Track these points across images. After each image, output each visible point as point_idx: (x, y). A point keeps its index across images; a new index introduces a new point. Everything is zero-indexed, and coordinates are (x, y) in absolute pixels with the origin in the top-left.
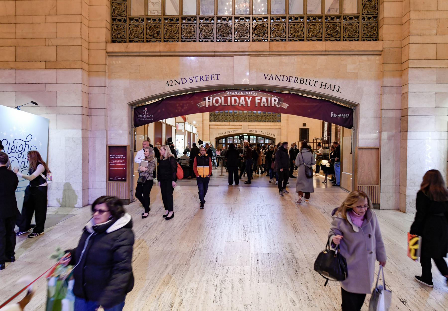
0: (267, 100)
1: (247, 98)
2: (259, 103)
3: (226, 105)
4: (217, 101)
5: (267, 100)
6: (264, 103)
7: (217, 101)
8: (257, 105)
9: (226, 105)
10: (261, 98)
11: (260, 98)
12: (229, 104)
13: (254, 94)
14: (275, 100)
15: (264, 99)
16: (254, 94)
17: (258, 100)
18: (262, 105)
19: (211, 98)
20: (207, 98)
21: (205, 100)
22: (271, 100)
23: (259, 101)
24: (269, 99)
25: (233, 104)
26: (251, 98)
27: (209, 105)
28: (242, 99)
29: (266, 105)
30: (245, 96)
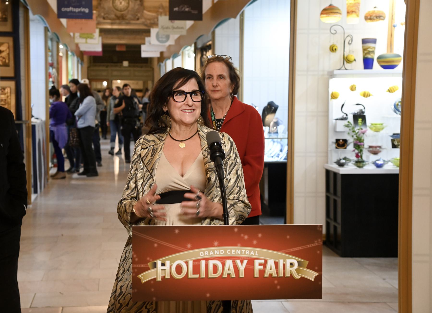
0: (277, 264)
1: (238, 262)
2: (262, 272)
4: (179, 269)
5: (277, 264)
6: (271, 272)
7: (179, 269)
8: (257, 275)
9: (197, 276)
10: (266, 261)
11: (263, 261)
13: (252, 253)
14: (292, 265)
15: (271, 263)
16: (252, 253)
17: (260, 264)
18: (267, 275)
19: (168, 263)
20: (159, 263)
21: (155, 266)
22: (284, 265)
23: (261, 267)
26: (245, 262)
27: (163, 278)
28: (229, 263)
30: (234, 258)
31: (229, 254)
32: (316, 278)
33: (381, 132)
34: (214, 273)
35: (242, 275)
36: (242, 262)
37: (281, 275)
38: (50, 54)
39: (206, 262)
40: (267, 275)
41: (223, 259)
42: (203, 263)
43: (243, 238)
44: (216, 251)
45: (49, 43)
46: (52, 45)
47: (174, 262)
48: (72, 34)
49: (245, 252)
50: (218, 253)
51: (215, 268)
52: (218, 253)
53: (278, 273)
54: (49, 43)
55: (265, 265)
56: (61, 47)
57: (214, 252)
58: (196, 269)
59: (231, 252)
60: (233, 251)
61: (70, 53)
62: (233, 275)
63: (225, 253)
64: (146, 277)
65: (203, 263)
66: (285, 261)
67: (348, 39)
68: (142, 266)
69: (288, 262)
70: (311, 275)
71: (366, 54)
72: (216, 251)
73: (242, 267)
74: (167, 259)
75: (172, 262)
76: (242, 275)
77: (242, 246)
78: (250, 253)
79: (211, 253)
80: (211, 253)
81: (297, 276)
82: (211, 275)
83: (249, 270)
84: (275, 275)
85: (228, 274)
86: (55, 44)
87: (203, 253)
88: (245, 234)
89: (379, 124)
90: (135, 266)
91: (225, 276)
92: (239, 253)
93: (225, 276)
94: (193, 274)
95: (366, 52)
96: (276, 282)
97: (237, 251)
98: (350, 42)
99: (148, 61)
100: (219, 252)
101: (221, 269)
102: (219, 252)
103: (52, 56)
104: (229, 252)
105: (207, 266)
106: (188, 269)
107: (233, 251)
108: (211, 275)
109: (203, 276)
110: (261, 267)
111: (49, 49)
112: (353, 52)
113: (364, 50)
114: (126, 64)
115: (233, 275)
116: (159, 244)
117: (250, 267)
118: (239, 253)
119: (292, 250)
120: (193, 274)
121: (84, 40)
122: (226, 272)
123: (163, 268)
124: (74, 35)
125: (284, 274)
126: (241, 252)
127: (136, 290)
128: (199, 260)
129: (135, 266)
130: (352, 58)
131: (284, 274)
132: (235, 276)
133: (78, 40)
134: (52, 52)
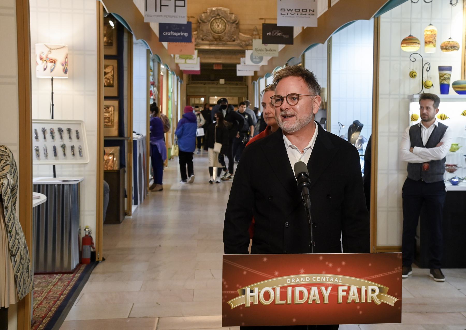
0: (359, 291)
1: (323, 288)
2: (345, 298)
3: (284, 302)
4: (267, 296)
5: (359, 291)
6: (354, 298)
7: (267, 296)
8: (340, 301)
9: (284, 302)
10: (349, 288)
11: (346, 288)
14: (373, 291)
15: (354, 289)
17: (344, 291)
19: (256, 290)
20: (248, 289)
21: (244, 292)
22: (366, 292)
23: (345, 294)
24: (363, 289)
26: (330, 288)
28: (314, 290)
30: (319, 285)
31: (314, 281)
32: (396, 303)
33: (457, 152)
34: (299, 300)
35: (326, 301)
36: (326, 289)
37: (363, 301)
38: (152, 73)
39: (292, 289)
40: (350, 301)
41: (308, 286)
42: (290, 290)
43: (328, 265)
44: (302, 278)
45: (151, 64)
46: (154, 66)
47: (262, 289)
48: (172, 55)
49: (329, 279)
50: (304, 280)
51: (301, 295)
52: (304, 280)
53: (360, 299)
54: (151, 64)
55: (348, 291)
56: (162, 66)
57: (300, 279)
58: (284, 295)
59: (316, 279)
60: (318, 278)
61: (170, 72)
62: (318, 301)
63: (311, 280)
64: (235, 303)
65: (290, 289)
66: (367, 287)
67: (427, 66)
68: (232, 292)
69: (370, 288)
70: (391, 301)
71: (442, 80)
72: (302, 278)
73: (326, 294)
74: (256, 286)
75: (260, 289)
76: (326, 301)
77: (327, 273)
78: (334, 280)
79: (298, 280)
80: (298, 280)
81: (378, 302)
82: (297, 301)
83: (333, 296)
84: (357, 301)
85: (313, 300)
86: (156, 64)
87: (290, 280)
88: (330, 262)
89: (455, 145)
90: (225, 292)
91: (310, 302)
92: (324, 280)
93: (310, 302)
94: (280, 300)
95: (442, 78)
96: (358, 307)
97: (322, 278)
98: (428, 69)
99: (243, 79)
100: (305, 280)
101: (307, 295)
102: (305, 280)
103: (153, 75)
104: (314, 279)
105: (293, 292)
106: (275, 296)
107: (318, 278)
108: (297, 301)
109: (290, 302)
110: (345, 294)
111: (151, 69)
112: (431, 78)
113: (441, 76)
114: (222, 81)
115: (318, 301)
116: (247, 271)
117: (334, 293)
118: (324, 280)
119: (373, 277)
120: (280, 300)
121: (183, 61)
122: (312, 298)
123: (252, 294)
124: (174, 56)
125: (366, 299)
126: (326, 279)
127: (226, 316)
128: (286, 287)
129: (225, 292)
130: (430, 84)
131: (366, 299)
132: (319, 302)
133: (178, 60)
134: (153, 72)
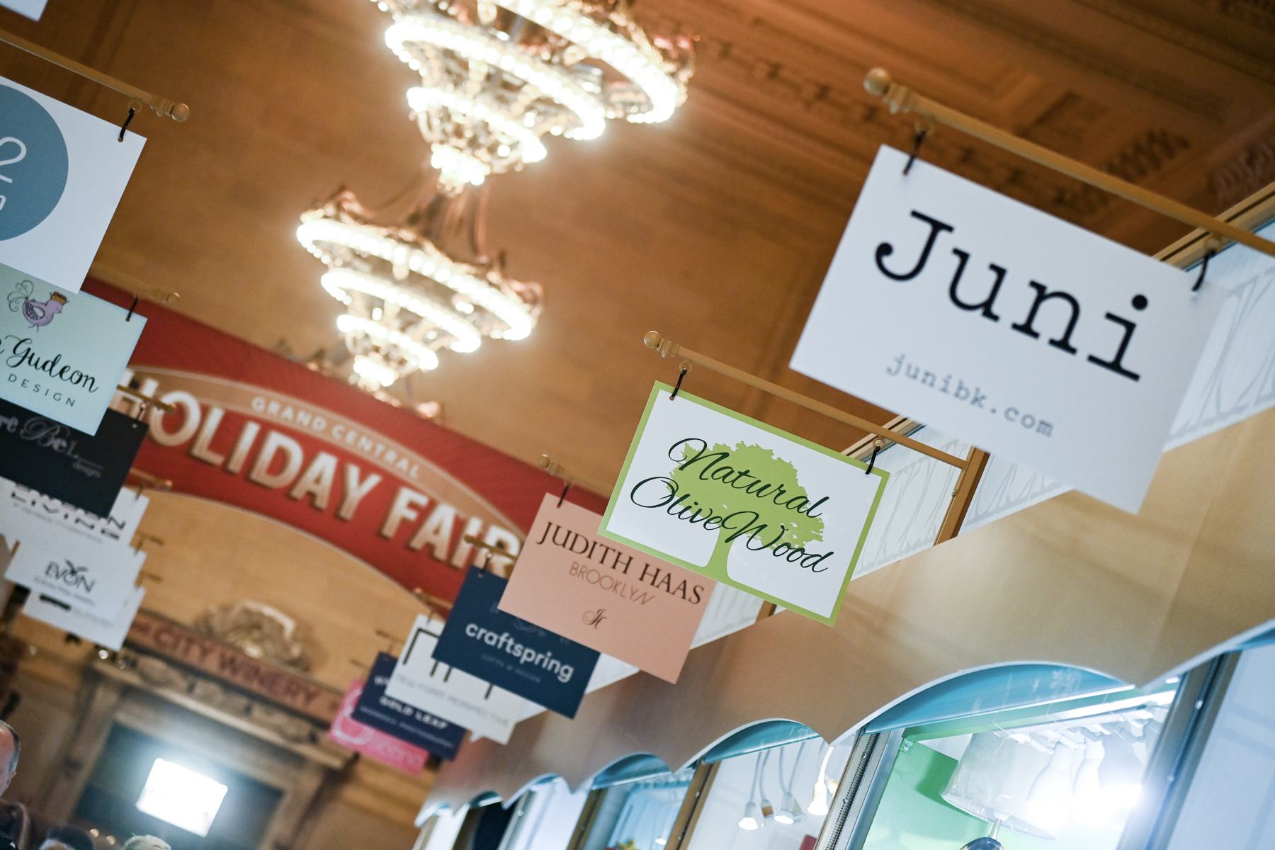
1: (353, 472)
2: (411, 529)
4: (175, 417)
5: (459, 525)
8: (390, 529)
10: (432, 505)
11: (422, 501)
12: (236, 465)
15: (444, 516)
17: (412, 506)
23: (412, 515)
24: (473, 528)
25: (260, 473)
26: (373, 480)
28: (325, 464)
29: (441, 554)
30: (345, 458)
35: (348, 511)
36: (362, 478)
41: (312, 446)
42: (251, 431)
55: (425, 512)
65: (251, 431)
73: (358, 488)
122: (307, 483)
